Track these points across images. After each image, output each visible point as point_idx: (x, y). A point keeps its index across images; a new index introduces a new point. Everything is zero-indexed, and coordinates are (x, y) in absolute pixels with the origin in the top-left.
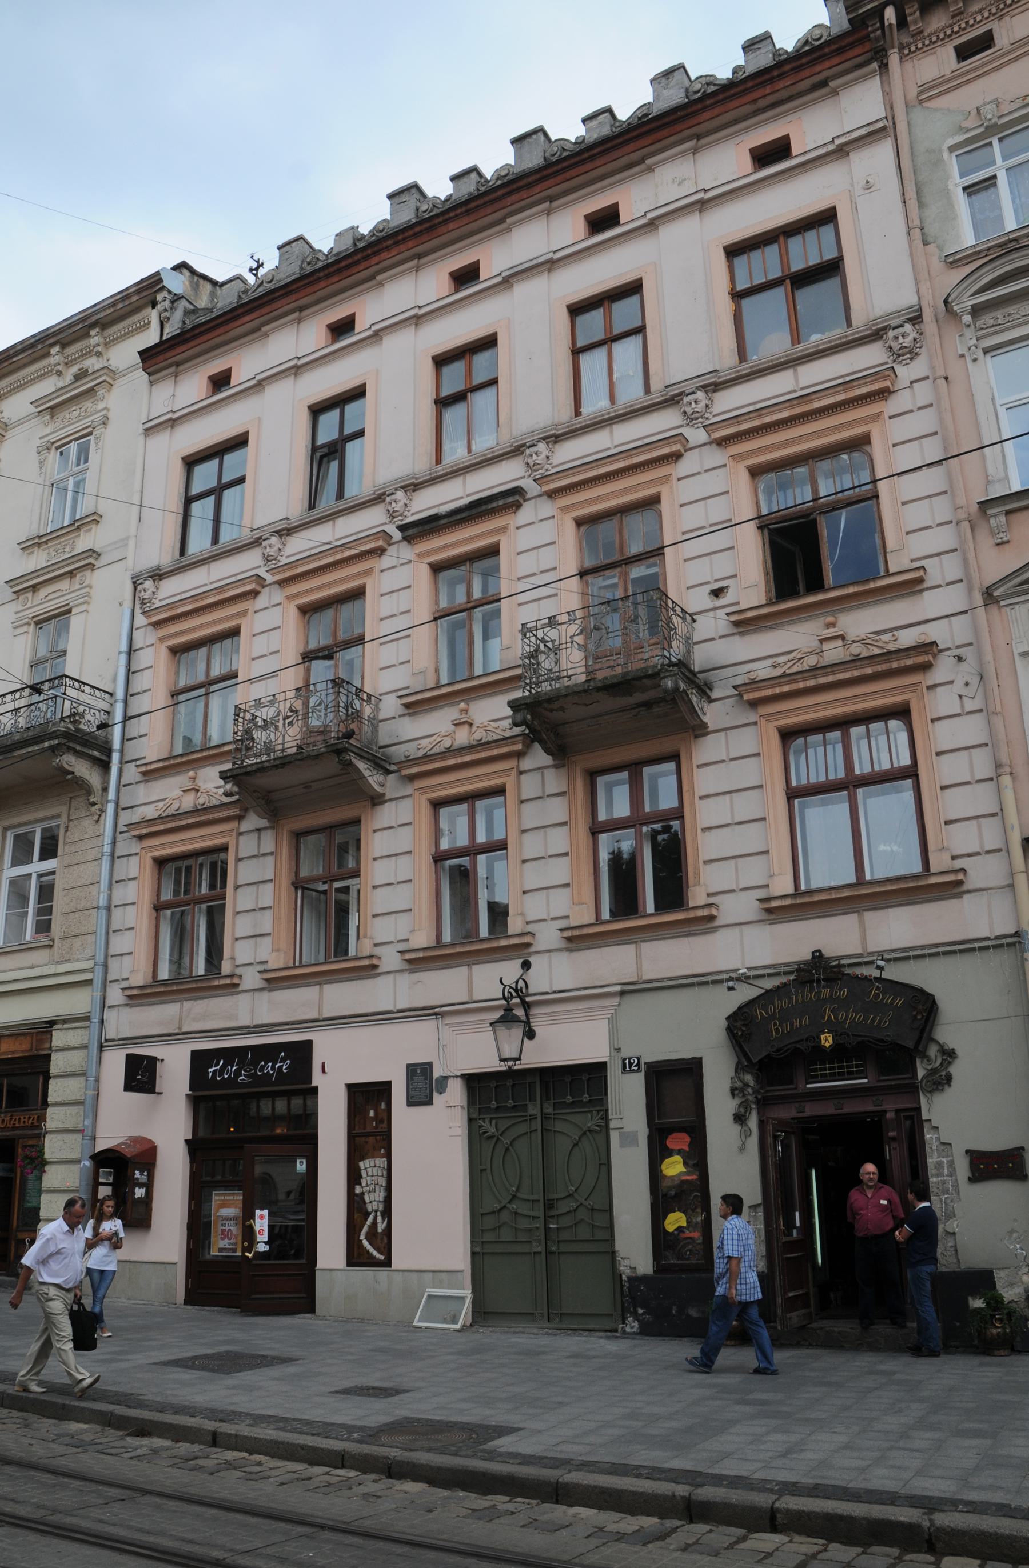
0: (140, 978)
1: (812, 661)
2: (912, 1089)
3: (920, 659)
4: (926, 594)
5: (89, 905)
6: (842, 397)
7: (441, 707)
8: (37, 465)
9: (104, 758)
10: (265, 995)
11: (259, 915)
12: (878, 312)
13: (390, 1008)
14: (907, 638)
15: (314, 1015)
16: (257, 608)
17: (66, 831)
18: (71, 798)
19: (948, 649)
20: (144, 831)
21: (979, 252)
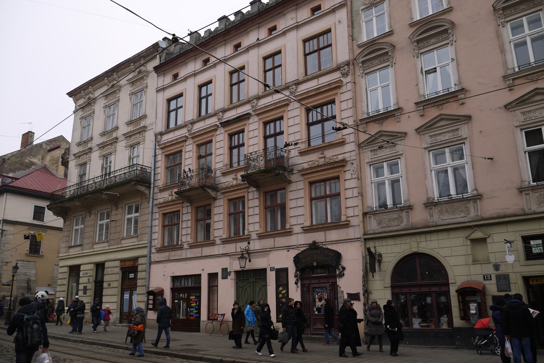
0: (159, 246)
1: (317, 163)
2: (335, 277)
3: (342, 164)
4: (345, 145)
5: (147, 226)
6: (328, 88)
7: (230, 174)
8: (129, 99)
9: (149, 186)
10: (189, 250)
11: (188, 229)
12: (339, 62)
13: (218, 254)
14: (340, 157)
15: (200, 255)
16: (187, 144)
17: (141, 205)
18: (142, 196)
19: (350, 161)
20: (160, 206)
21: (366, 44)
